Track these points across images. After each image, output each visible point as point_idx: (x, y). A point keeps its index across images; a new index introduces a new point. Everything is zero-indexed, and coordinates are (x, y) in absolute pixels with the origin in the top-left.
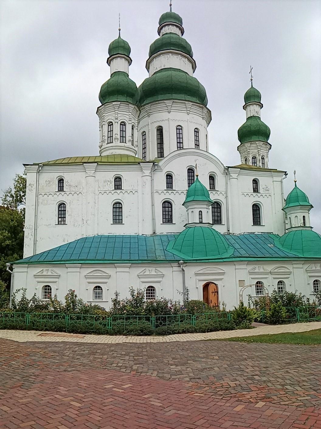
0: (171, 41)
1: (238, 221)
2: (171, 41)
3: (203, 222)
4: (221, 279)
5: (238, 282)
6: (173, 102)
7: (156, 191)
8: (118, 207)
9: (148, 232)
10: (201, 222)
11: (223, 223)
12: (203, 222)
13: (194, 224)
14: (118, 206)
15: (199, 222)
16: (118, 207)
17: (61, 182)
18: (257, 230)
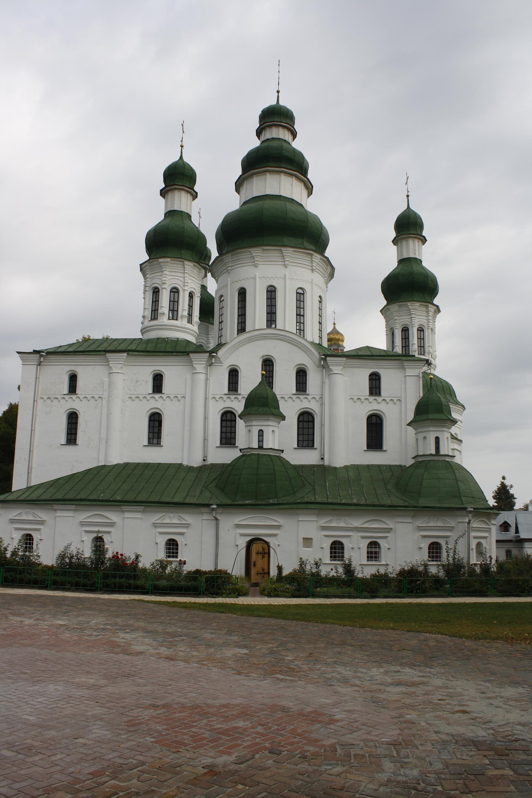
0: (274, 151)
1: (344, 446)
2: (274, 151)
3: (264, 447)
4: (275, 535)
5: (301, 540)
6: (263, 249)
7: (213, 396)
8: (155, 421)
9: (196, 461)
10: (261, 447)
11: (315, 447)
12: (264, 447)
13: (249, 450)
14: (229, 416)
15: (257, 447)
16: (155, 421)
17: (301, 374)
18: (375, 458)
